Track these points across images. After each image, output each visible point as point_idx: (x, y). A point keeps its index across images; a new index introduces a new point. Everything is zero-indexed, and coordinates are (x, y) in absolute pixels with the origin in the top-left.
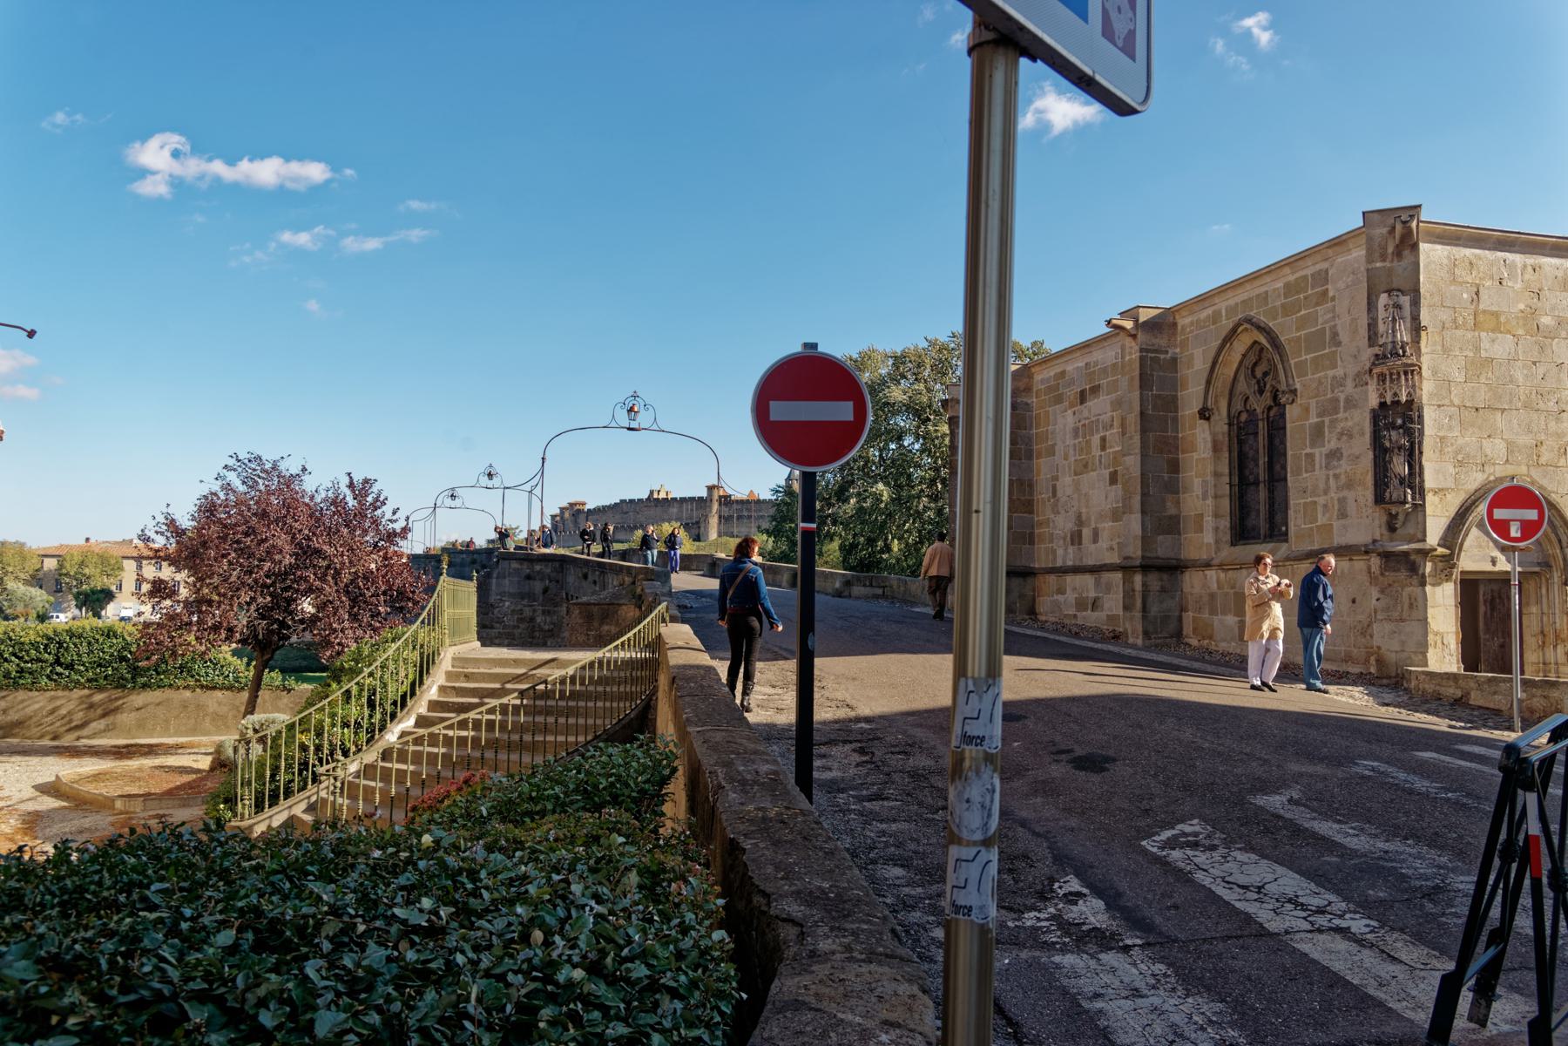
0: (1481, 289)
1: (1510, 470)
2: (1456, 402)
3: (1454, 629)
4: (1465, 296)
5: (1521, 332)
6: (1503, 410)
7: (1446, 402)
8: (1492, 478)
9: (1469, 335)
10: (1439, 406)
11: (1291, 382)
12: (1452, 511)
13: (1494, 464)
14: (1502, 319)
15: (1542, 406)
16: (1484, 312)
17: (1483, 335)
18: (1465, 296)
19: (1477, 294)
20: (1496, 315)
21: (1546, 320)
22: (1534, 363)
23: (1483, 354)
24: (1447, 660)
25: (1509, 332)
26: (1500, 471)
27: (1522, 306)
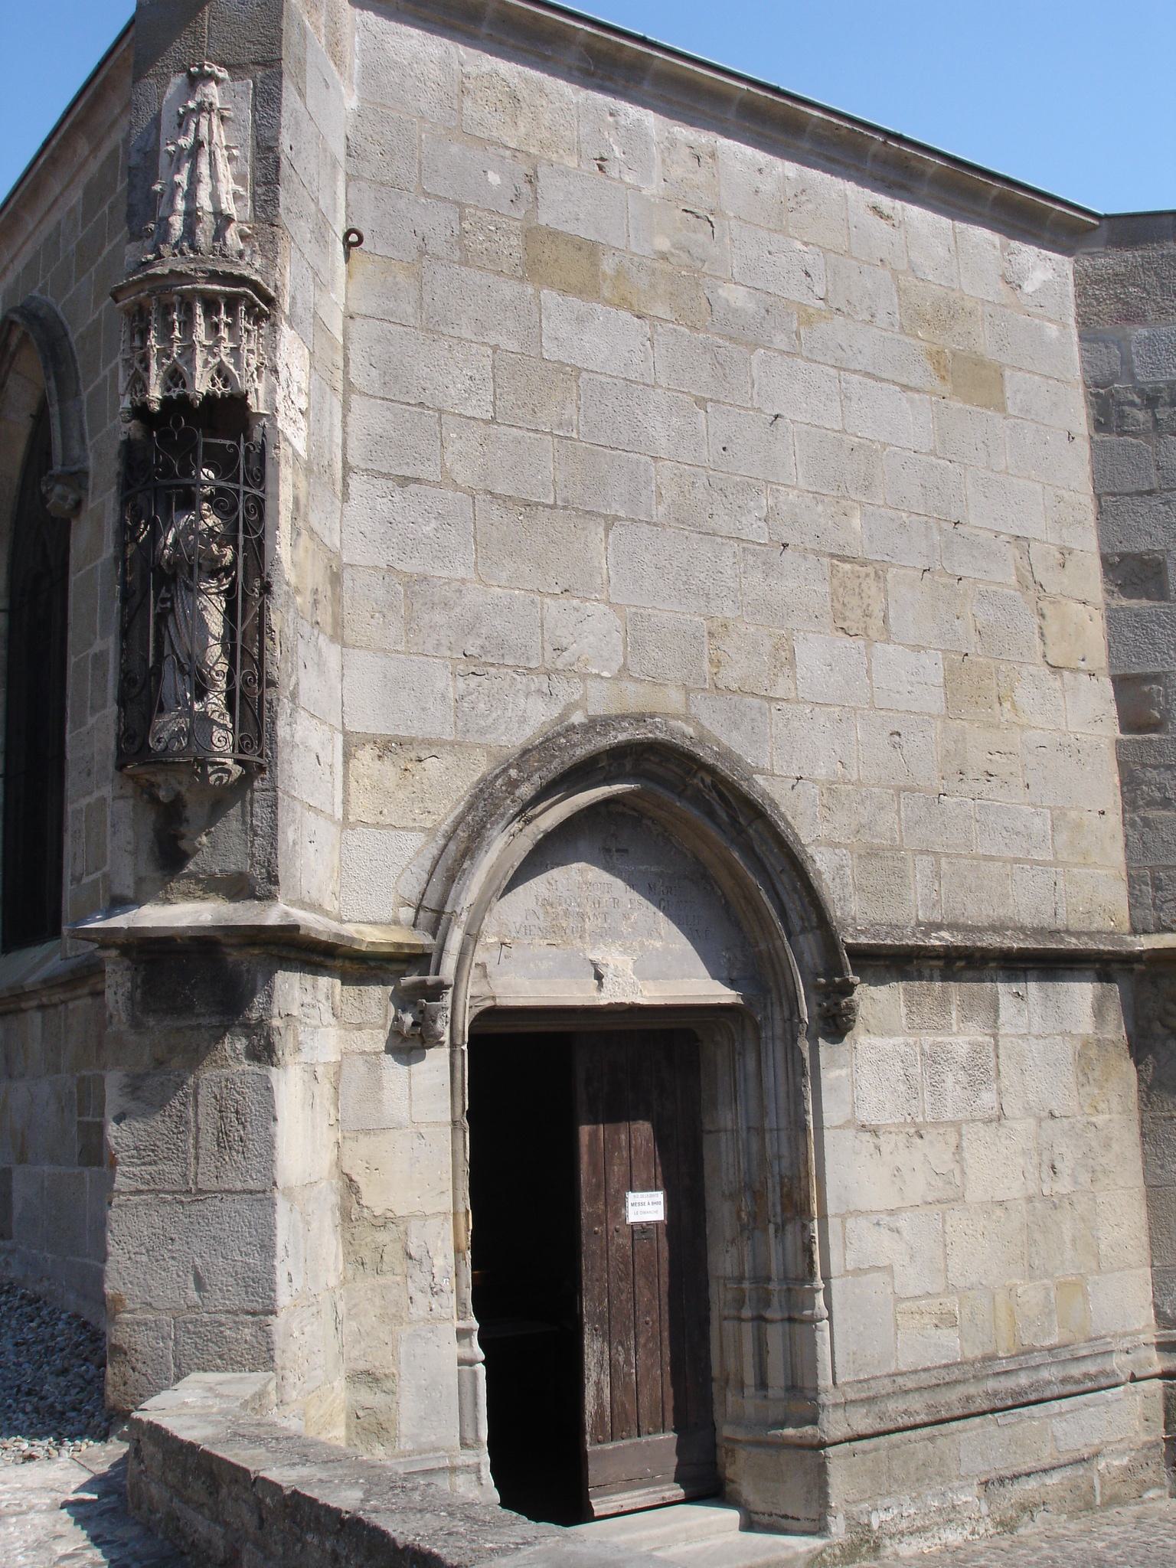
0: (543, 171)
1: (634, 697)
2: (464, 475)
3: (448, 1203)
4: (494, 178)
5: (661, 310)
6: (610, 522)
7: (430, 471)
8: (577, 718)
9: (508, 290)
10: (404, 481)
11: (76, 451)
12: (445, 810)
13: (584, 677)
14: (608, 265)
15: (723, 523)
16: (554, 234)
17: (549, 296)
18: (494, 178)
19: (531, 180)
20: (590, 250)
21: (734, 295)
22: (701, 402)
23: (551, 351)
24: (418, 1311)
25: (624, 303)
26: (600, 701)
27: (663, 244)
